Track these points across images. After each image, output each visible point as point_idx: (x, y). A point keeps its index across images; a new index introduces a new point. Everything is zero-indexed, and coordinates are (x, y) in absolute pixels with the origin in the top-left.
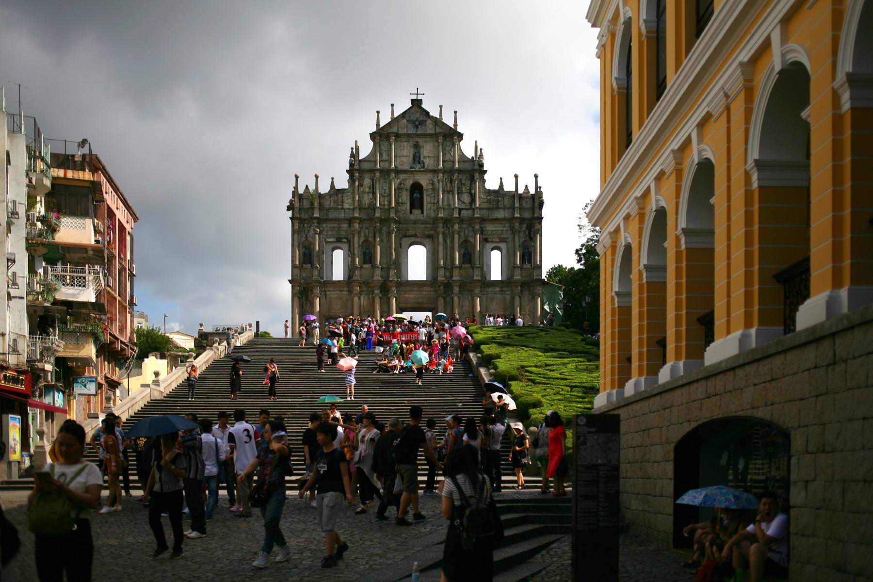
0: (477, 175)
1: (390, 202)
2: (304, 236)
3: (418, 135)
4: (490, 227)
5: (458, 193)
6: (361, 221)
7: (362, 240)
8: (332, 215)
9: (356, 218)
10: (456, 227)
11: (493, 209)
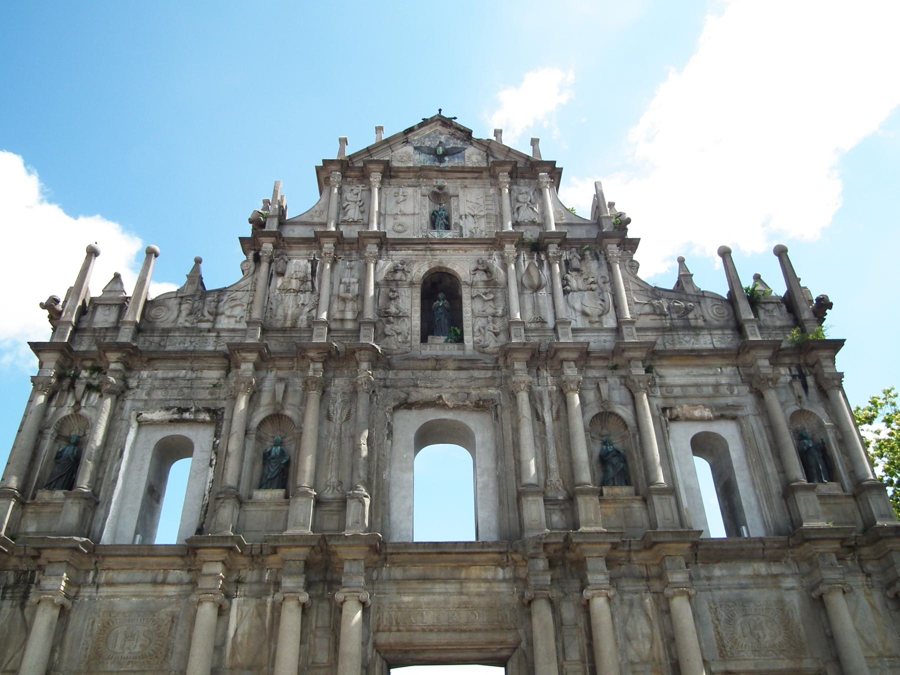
0: (613, 249)
1: (360, 313)
2: (71, 402)
3: (442, 171)
4: (674, 376)
5: (566, 292)
6: (265, 359)
7: (261, 414)
8: (175, 344)
9: (249, 348)
10: (571, 372)
11: (673, 329)
